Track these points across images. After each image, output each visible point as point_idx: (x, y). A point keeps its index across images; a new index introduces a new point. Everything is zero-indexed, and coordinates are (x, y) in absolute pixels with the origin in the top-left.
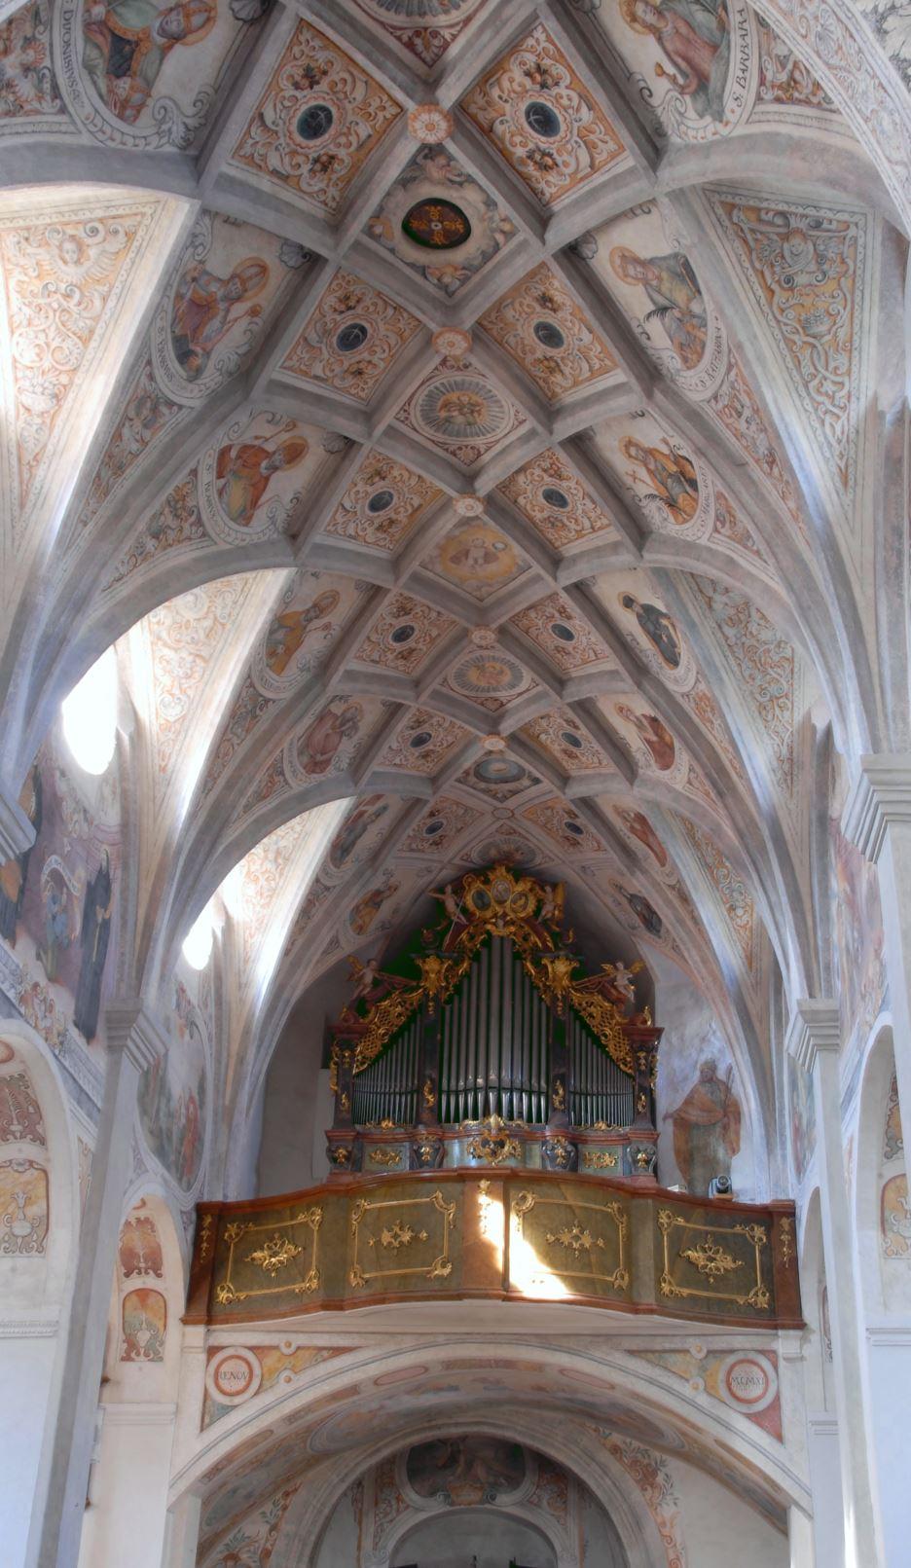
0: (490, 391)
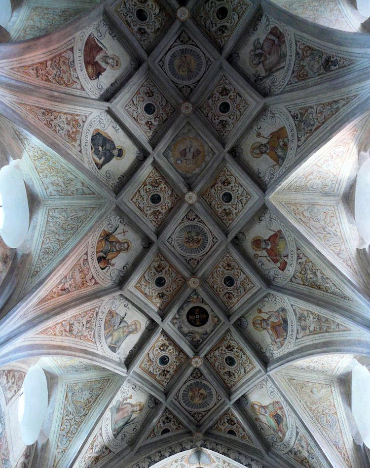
0: (182, 250)
